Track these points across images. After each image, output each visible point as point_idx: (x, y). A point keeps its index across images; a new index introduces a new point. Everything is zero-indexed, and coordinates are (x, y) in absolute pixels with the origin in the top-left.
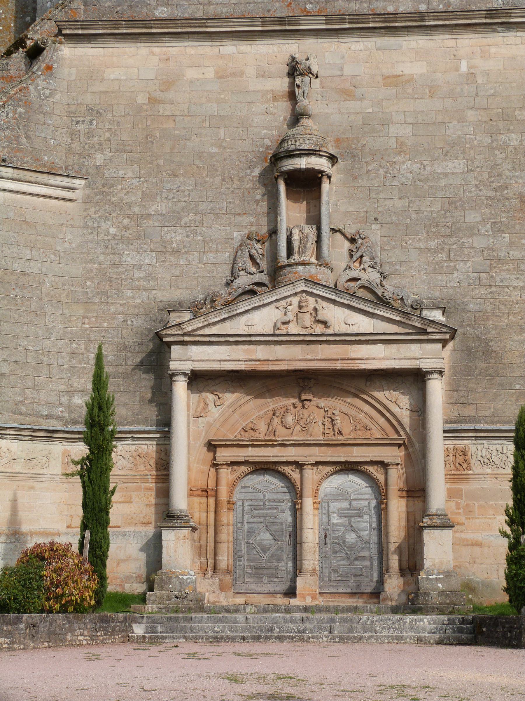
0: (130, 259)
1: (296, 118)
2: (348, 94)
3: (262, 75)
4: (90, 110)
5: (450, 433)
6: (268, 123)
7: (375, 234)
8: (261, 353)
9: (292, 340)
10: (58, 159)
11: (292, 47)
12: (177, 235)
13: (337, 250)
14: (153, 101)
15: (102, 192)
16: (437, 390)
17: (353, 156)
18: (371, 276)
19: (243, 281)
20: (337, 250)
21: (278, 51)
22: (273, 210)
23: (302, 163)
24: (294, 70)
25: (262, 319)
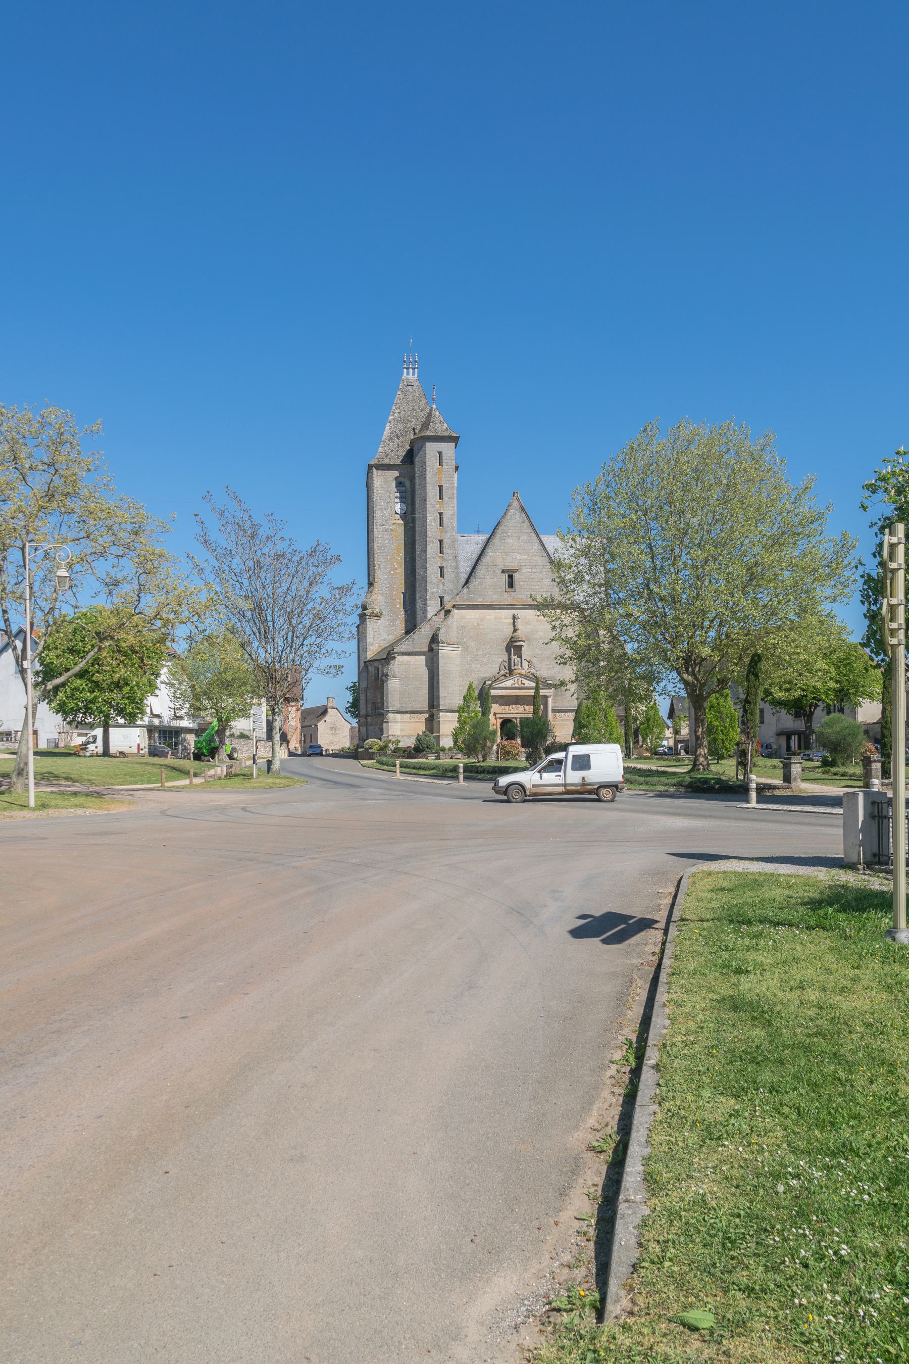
0: (474, 666)
1: (515, 631)
2: (527, 623)
3: (506, 618)
4: (462, 627)
5: (553, 711)
6: (508, 631)
7: (534, 660)
8: (508, 691)
9: (516, 688)
10: (454, 640)
11: (513, 611)
12: (485, 660)
13: (525, 664)
14: (478, 625)
15: (466, 648)
16: (550, 699)
17: (529, 640)
18: (533, 671)
19: (502, 672)
20: (525, 664)
21: (510, 613)
22: (510, 655)
23: (518, 644)
24: (514, 618)
25: (509, 683)
